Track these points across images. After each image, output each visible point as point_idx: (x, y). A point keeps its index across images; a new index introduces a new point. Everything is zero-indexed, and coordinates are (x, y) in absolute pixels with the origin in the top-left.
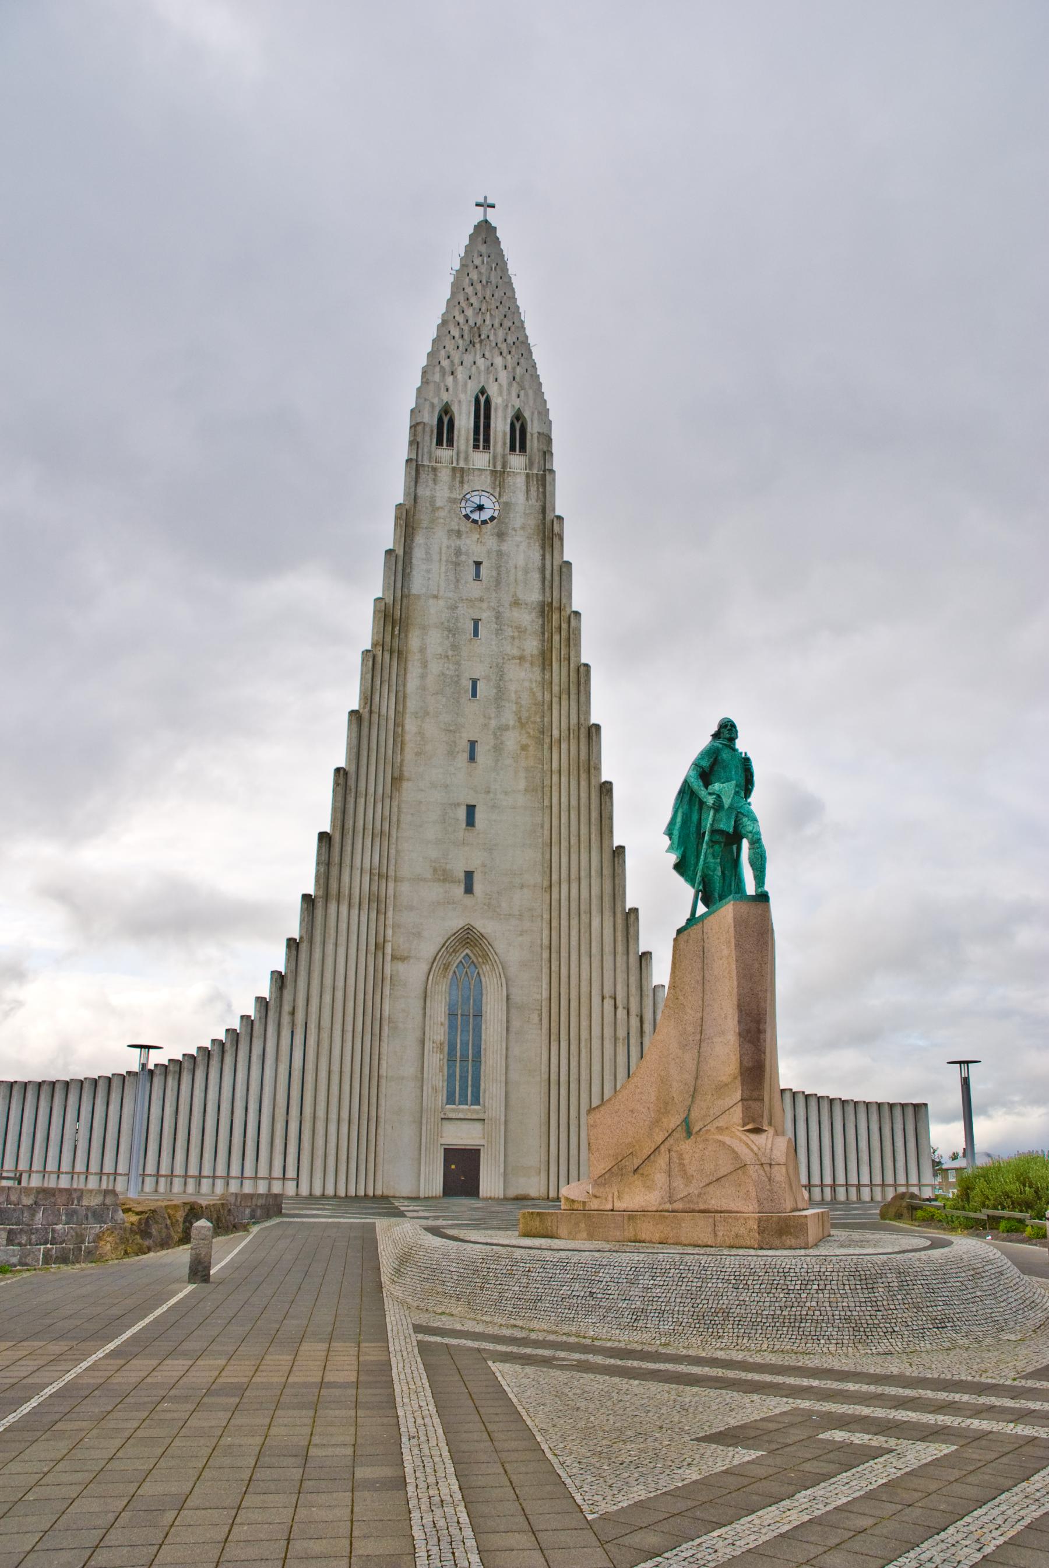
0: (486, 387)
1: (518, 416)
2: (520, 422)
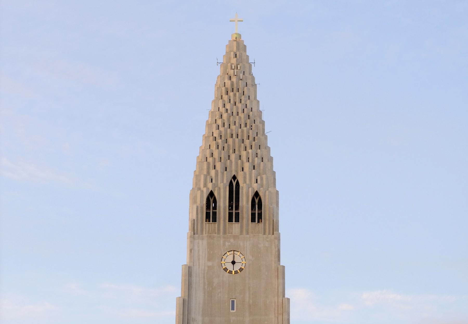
0: (236, 175)
1: (257, 194)
2: (258, 198)
